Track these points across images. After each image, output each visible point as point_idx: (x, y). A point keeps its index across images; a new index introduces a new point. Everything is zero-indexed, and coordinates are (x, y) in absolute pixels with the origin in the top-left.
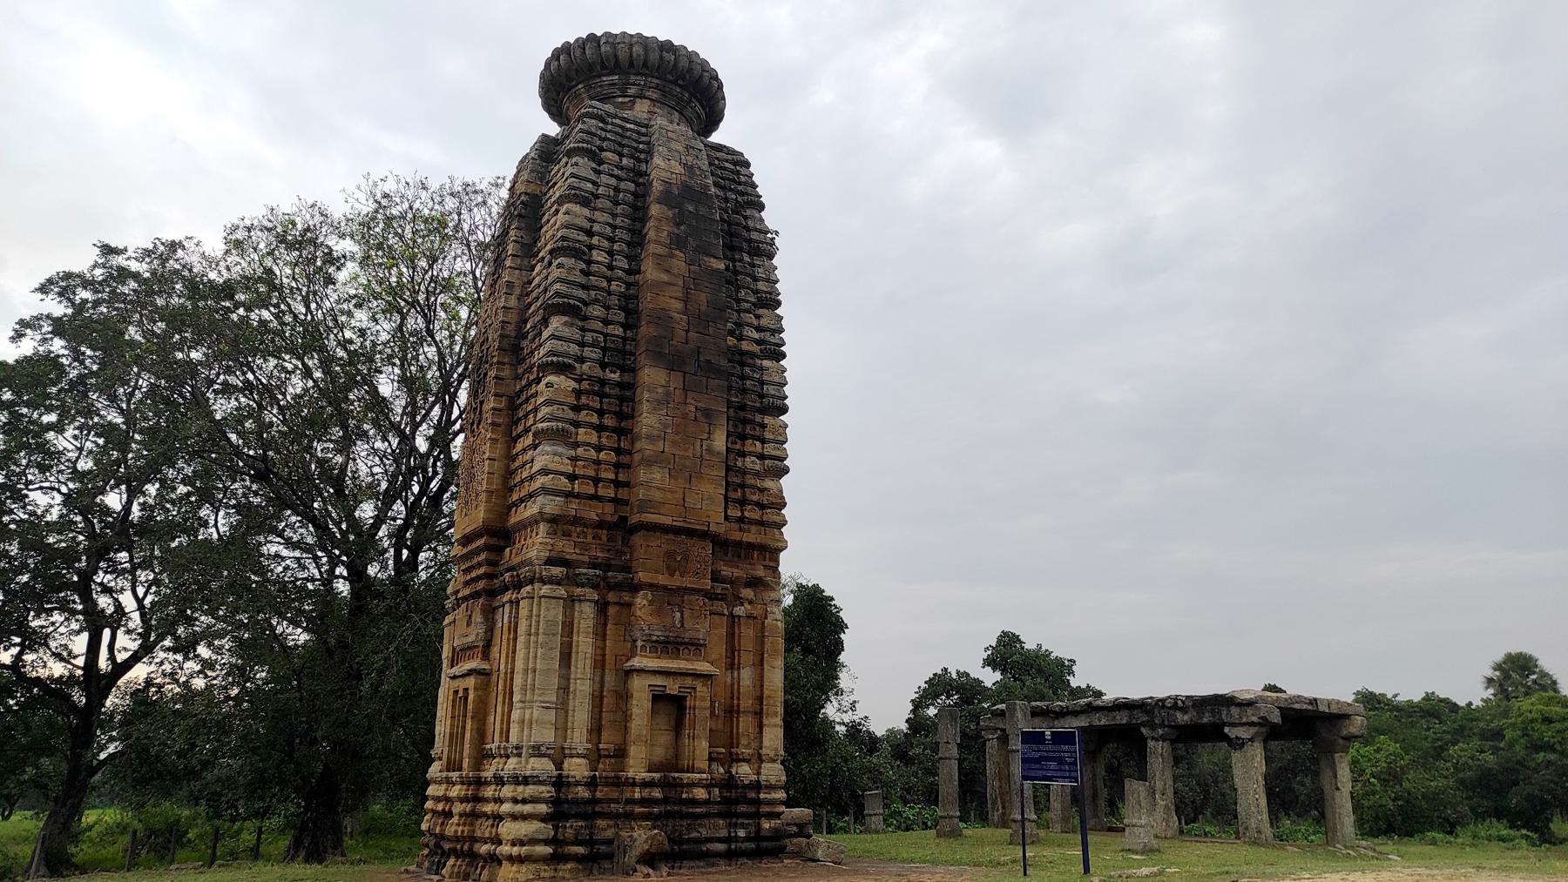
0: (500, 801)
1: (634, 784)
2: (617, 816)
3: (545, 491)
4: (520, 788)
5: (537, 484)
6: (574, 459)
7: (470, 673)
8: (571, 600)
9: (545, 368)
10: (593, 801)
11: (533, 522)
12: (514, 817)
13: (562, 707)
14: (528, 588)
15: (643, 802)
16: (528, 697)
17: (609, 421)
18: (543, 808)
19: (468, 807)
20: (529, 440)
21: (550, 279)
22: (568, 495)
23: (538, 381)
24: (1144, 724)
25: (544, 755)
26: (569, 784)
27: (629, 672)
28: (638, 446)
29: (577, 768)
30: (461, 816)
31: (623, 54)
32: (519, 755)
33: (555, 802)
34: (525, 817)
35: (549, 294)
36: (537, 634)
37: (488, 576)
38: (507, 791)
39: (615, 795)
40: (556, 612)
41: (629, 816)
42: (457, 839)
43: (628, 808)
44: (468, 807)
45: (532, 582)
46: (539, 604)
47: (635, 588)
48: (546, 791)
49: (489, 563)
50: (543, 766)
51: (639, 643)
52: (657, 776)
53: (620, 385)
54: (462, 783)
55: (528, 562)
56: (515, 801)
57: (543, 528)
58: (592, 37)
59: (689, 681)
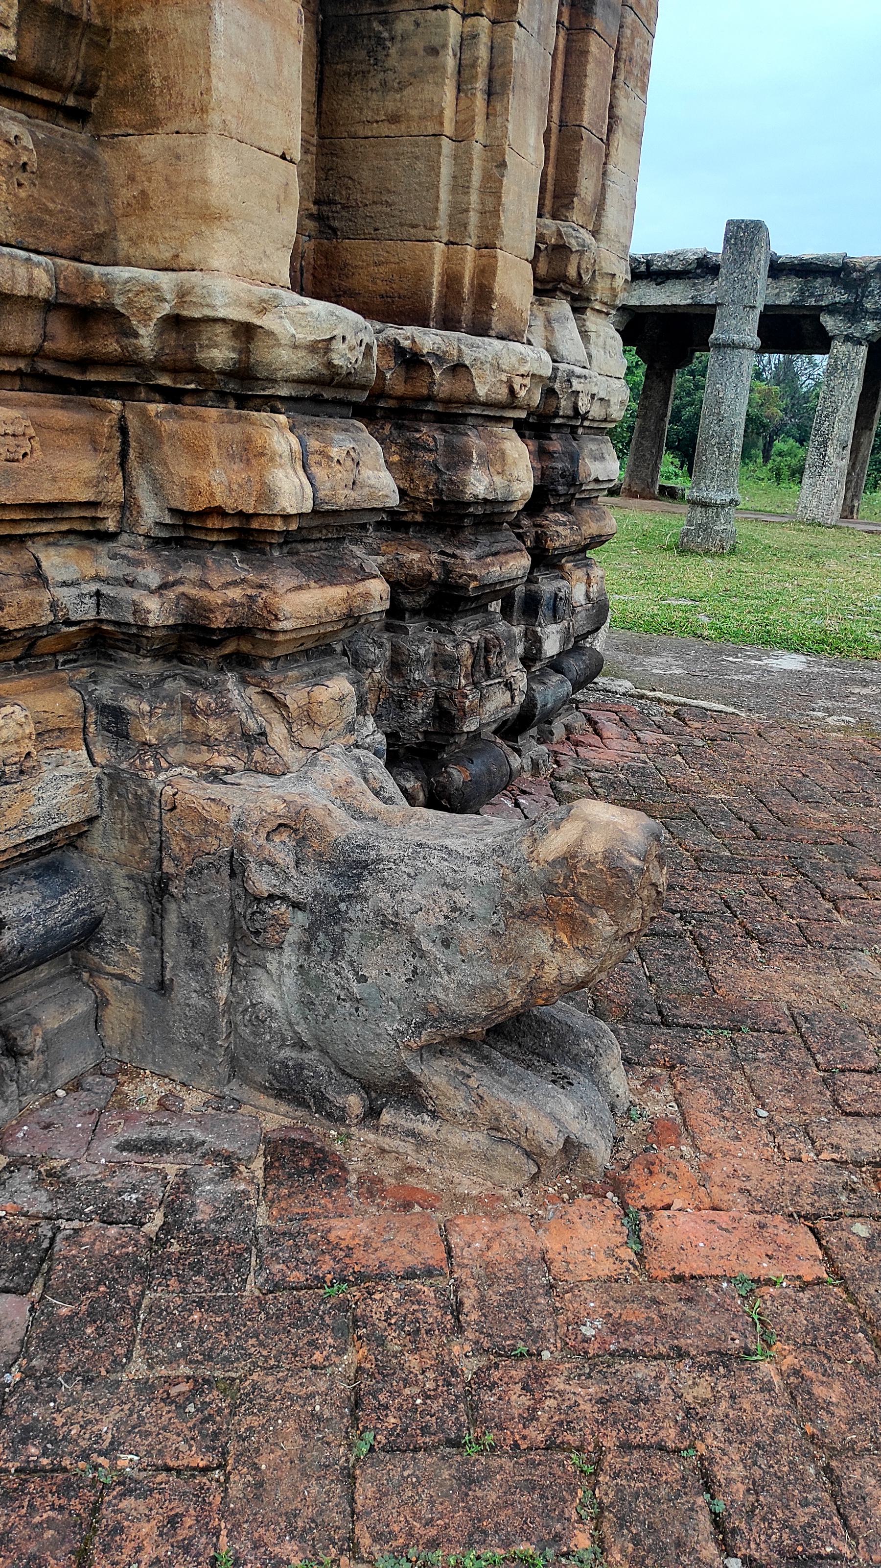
2: (102, 642)
15: (322, 537)
24: (832, 309)
39: (72, 472)
43: (223, 586)
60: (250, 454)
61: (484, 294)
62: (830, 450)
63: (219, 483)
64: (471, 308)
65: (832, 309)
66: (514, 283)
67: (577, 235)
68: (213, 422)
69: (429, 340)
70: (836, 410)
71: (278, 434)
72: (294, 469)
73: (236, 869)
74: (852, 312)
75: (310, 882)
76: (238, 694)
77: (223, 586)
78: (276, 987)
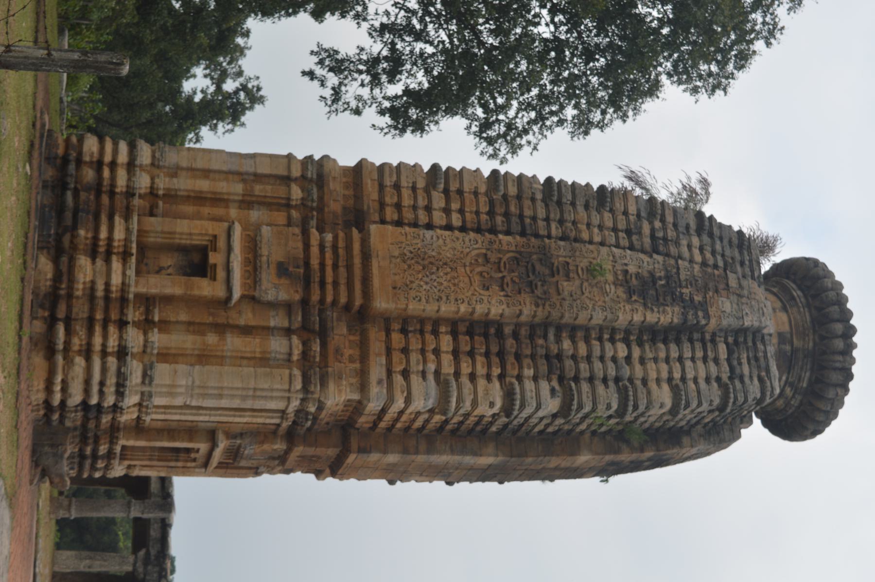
0: (104, 353)
1: (112, 442)
3: (391, 399)
4: (113, 389)
5: (398, 379)
6: (418, 414)
7: (229, 289)
8: (283, 412)
9: (509, 395)
10: (98, 419)
11: (363, 387)
12: (87, 382)
13: (186, 407)
14: (298, 385)
16: (197, 391)
17: (449, 427)
18: (94, 401)
19: (100, 293)
20: (448, 368)
21: (600, 389)
22: (384, 411)
23: (501, 377)
24: (148, 553)
25: (142, 399)
26: (114, 411)
27: (212, 436)
28: (423, 446)
29: (127, 417)
30: (93, 282)
31: (821, 405)
32: (143, 383)
33: (99, 406)
34: (87, 391)
35: (585, 387)
36: (254, 397)
37: (322, 301)
38: (112, 361)
40: (273, 405)
41: (84, 440)
42: (72, 281)
43: (91, 441)
44: (100, 293)
45: (305, 389)
46: (282, 397)
47: (291, 437)
48: (110, 400)
49: (335, 303)
50: (131, 399)
51: (238, 442)
52: (118, 449)
53: (485, 431)
54: (123, 283)
55: (323, 383)
56: (102, 384)
57: (356, 397)
58: (850, 377)
59: (201, 460)
60: (105, 444)
61: (125, 459)
62: (87, 561)
63: (102, 441)
64: (123, 457)
65: (148, 553)
66: (127, 463)
67: (137, 468)
68: (108, 440)
69: (118, 455)
70: (105, 561)
71: (107, 446)
72: (103, 449)
73: (61, 444)
74: (147, 561)
75: (60, 452)
76: (77, 440)
77: (91, 441)
78: (47, 449)
